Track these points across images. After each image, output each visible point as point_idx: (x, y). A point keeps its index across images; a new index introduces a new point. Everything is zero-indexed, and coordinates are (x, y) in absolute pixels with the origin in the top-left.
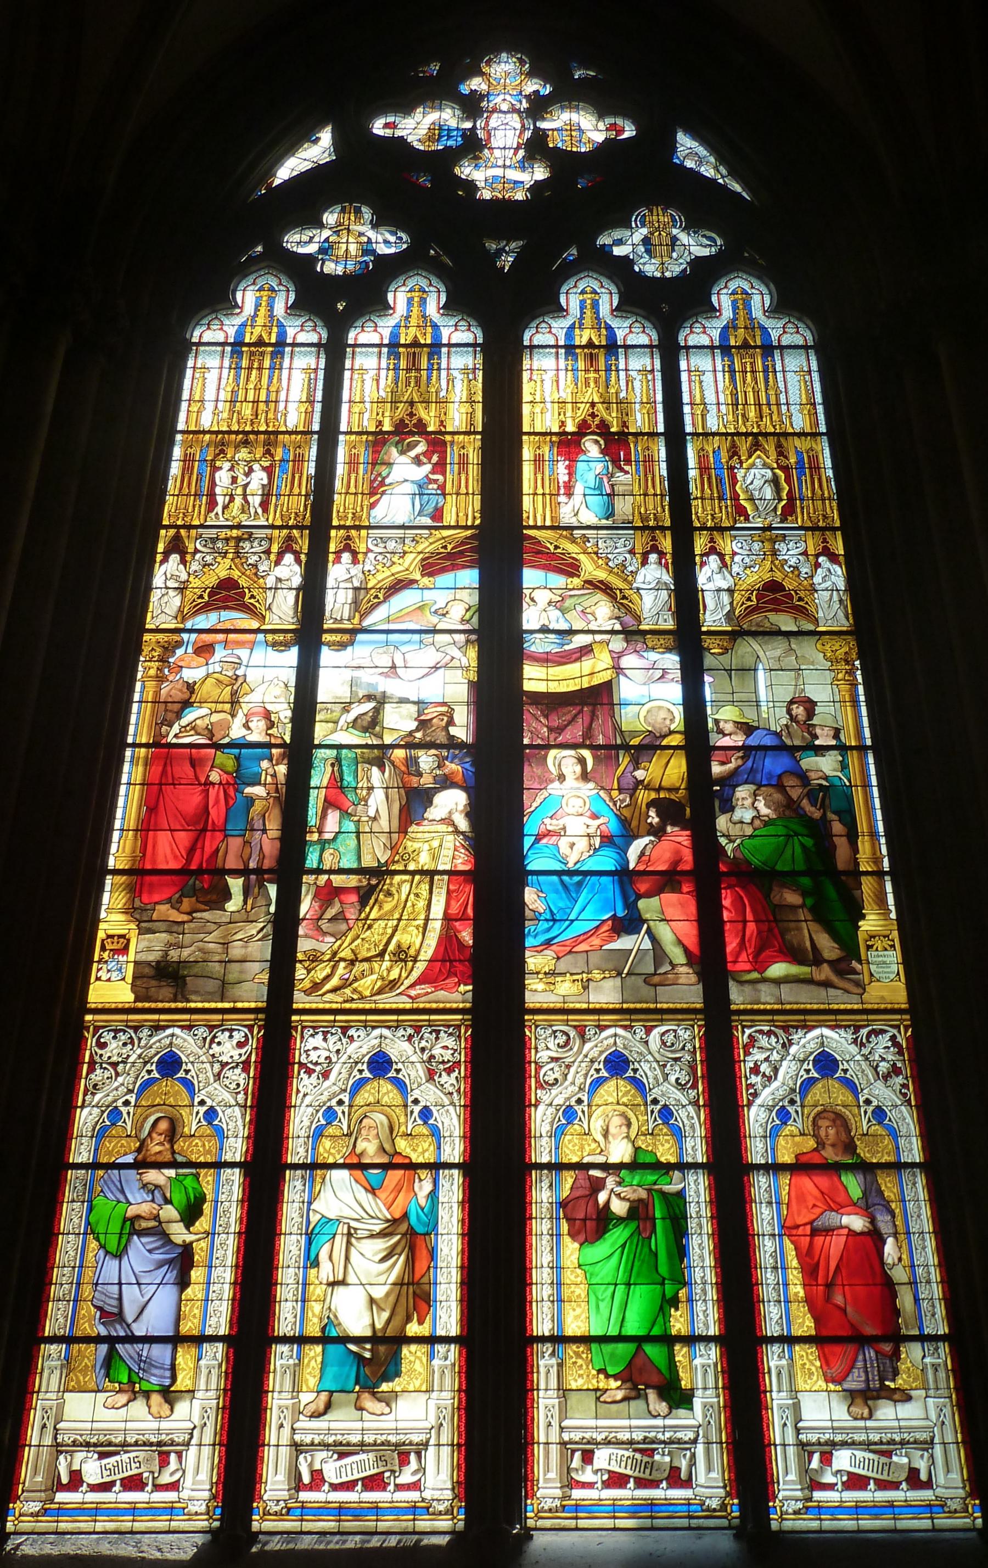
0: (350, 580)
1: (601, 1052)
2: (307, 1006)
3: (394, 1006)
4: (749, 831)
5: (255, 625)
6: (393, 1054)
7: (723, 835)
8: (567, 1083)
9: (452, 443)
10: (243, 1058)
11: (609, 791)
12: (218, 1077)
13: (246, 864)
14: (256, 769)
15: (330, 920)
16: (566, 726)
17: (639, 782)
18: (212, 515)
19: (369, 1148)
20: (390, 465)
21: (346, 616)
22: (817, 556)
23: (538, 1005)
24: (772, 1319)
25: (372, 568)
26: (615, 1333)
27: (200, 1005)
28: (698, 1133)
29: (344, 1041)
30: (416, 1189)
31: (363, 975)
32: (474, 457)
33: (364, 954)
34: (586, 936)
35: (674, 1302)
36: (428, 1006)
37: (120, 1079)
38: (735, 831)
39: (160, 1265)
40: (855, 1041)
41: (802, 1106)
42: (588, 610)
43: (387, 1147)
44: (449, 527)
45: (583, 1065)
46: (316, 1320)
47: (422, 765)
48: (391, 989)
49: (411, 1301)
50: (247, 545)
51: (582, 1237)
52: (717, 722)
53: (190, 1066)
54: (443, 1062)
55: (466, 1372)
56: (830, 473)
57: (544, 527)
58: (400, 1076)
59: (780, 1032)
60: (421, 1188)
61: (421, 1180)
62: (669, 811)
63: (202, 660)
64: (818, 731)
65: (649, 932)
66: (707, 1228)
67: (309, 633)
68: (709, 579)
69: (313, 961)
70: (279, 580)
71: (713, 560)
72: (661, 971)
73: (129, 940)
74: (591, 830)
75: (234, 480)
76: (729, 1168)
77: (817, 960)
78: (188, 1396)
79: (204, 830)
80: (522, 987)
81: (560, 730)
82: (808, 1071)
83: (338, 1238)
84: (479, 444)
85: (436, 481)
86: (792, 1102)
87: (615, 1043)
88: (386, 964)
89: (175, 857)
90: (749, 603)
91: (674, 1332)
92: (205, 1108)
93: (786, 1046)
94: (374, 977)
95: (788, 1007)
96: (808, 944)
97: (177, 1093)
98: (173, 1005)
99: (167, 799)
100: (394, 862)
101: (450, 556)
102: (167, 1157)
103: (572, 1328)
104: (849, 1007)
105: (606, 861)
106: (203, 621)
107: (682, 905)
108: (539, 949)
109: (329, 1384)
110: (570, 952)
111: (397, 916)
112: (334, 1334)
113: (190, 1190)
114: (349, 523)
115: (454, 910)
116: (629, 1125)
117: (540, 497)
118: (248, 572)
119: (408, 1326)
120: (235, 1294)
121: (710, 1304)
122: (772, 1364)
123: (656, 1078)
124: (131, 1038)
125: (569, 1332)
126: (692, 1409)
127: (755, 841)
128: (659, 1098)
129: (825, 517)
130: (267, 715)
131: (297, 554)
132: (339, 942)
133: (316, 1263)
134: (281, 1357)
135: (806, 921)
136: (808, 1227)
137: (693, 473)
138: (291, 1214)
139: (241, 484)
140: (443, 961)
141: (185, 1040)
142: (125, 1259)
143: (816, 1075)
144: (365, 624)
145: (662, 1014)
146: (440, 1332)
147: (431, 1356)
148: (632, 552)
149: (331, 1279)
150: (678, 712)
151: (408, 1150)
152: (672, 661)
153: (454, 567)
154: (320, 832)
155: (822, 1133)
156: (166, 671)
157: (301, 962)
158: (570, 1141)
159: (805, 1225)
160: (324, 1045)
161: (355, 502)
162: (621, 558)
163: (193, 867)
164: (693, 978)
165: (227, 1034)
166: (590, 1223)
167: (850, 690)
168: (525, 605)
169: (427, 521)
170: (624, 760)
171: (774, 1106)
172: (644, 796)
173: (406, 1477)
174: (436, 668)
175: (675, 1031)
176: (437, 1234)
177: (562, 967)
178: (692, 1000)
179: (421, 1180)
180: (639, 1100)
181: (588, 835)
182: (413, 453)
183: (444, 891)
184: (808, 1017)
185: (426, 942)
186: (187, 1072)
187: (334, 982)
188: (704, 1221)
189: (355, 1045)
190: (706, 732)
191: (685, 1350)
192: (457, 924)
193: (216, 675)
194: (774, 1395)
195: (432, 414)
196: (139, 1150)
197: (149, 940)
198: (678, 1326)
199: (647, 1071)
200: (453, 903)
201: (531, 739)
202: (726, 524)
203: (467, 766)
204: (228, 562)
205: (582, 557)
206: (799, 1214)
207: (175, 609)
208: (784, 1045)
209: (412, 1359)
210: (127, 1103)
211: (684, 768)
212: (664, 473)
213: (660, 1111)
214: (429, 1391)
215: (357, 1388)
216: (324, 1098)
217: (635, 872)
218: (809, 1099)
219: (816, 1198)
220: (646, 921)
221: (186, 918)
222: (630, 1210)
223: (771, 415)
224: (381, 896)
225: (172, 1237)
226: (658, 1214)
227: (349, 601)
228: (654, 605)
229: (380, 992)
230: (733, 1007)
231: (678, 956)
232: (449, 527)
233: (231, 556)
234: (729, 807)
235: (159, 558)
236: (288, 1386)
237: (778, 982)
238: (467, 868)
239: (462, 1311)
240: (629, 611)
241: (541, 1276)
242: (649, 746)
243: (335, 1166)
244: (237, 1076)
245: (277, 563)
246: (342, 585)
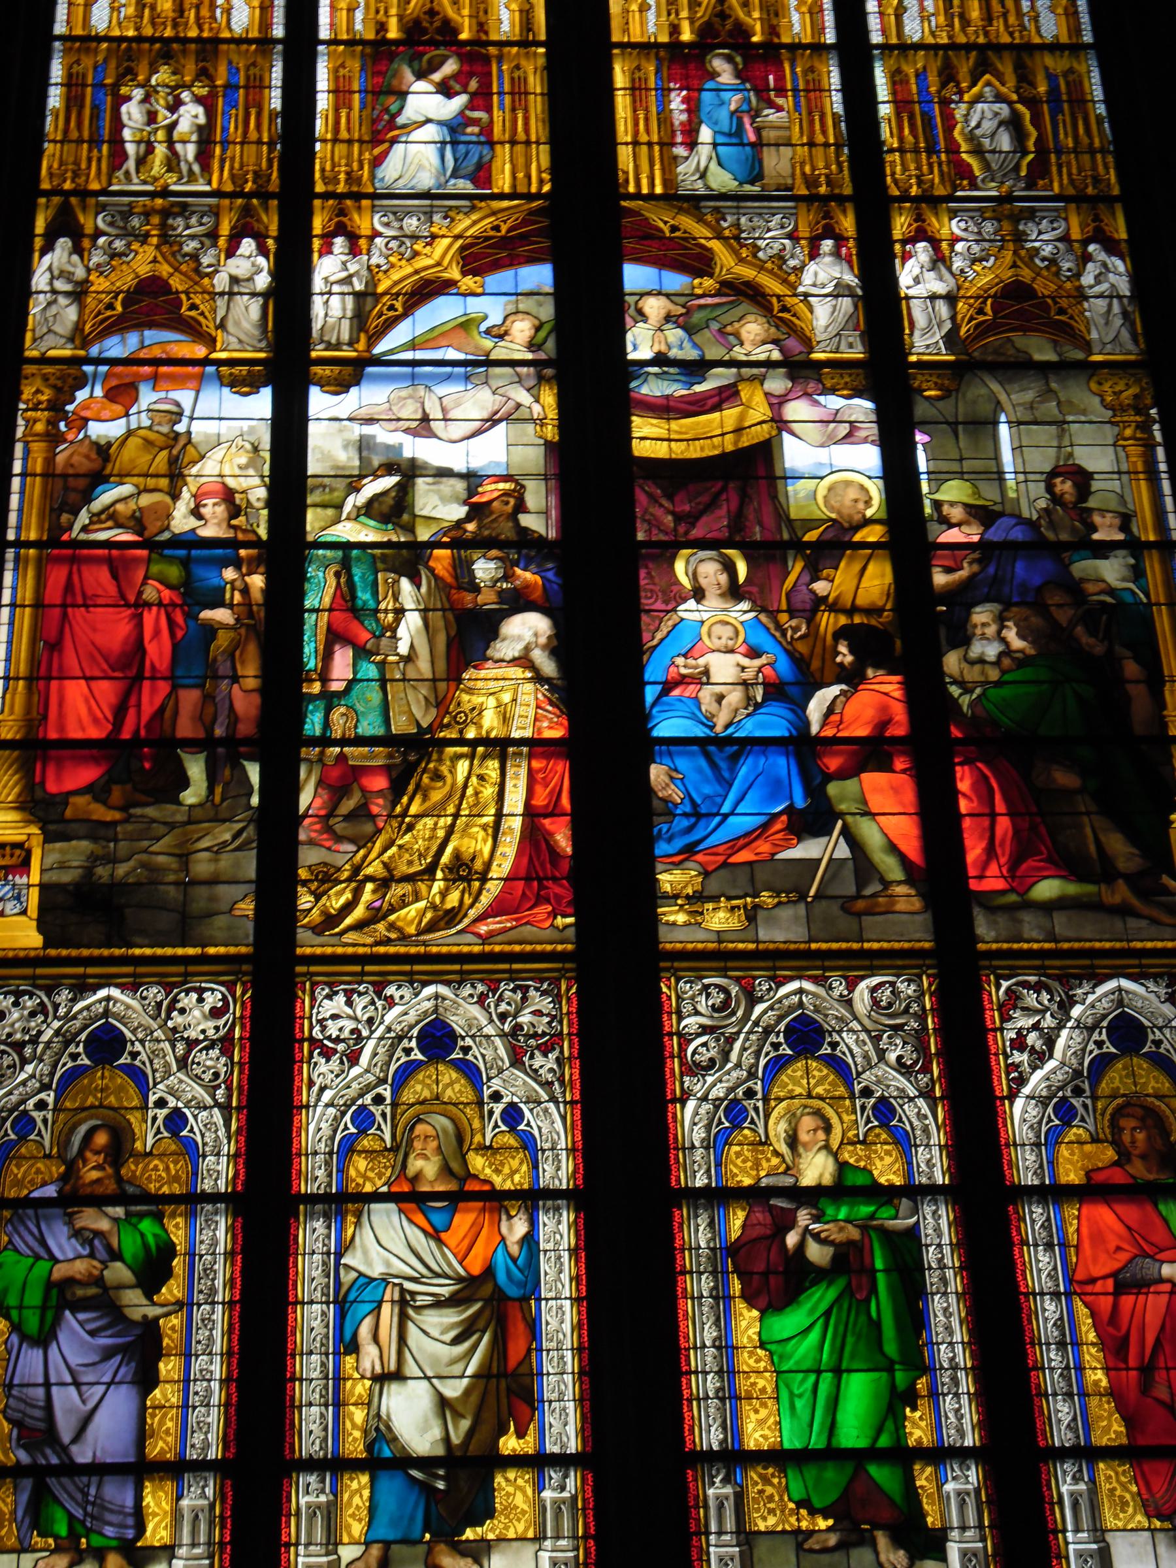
0: (347, 281)
1: (780, 1018)
2: (319, 951)
3: (455, 949)
4: (994, 674)
5: (200, 351)
6: (457, 1022)
7: (954, 682)
8: (729, 1065)
9: (500, 59)
10: (222, 1033)
11: (773, 614)
12: (183, 1063)
13: (210, 730)
14: (215, 581)
15: (348, 817)
16: (702, 513)
17: (819, 601)
18: (120, 174)
19: (426, 1166)
20: (403, 95)
21: (345, 336)
22: (1085, 243)
23: (679, 946)
25: (382, 261)
26: (821, 1445)
27: (148, 951)
28: (934, 1140)
29: (379, 1004)
30: (504, 1230)
31: (404, 904)
32: (536, 83)
33: (403, 869)
34: (748, 838)
35: (910, 1398)
36: (507, 948)
37: (29, 1068)
38: (972, 674)
39: (107, 1354)
41: (1095, 1098)
42: (729, 329)
43: (455, 1166)
44: (501, 196)
45: (753, 1037)
46: (357, 1434)
47: (479, 574)
48: (450, 924)
49: (504, 1401)
50: (179, 222)
51: (763, 1301)
52: (937, 505)
53: (138, 1047)
54: (535, 1036)
55: (596, 1509)
56: (1101, 109)
57: (651, 197)
58: (469, 1057)
59: (1055, 985)
60: (510, 1228)
61: (510, 1217)
62: (872, 644)
63: (119, 409)
64: (1097, 519)
66: (955, 1284)
67: (288, 366)
68: (917, 281)
69: (323, 882)
70: (234, 280)
71: (922, 250)
72: (868, 891)
73: (29, 853)
74: (749, 675)
75: (152, 117)
76: (983, 1191)
77: (1105, 872)
78: (164, 1555)
79: (139, 678)
80: (653, 920)
81: (692, 519)
82: (1099, 1044)
83: (386, 1309)
84: (541, 61)
85: (476, 122)
86: (1078, 1092)
87: (801, 1004)
88: (438, 885)
89: (96, 721)
90: (982, 318)
91: (911, 1442)
92: (165, 1111)
93: (1065, 1006)
94: (422, 904)
95: (1066, 945)
96: (1092, 848)
97: (121, 1088)
98: (106, 952)
99: (77, 629)
100: (442, 727)
101: (505, 243)
102: (111, 1187)
103: (756, 1436)
104: (1160, 945)
105: (773, 723)
106: (115, 347)
107: (896, 790)
109: (383, 1531)
110: (725, 865)
111: (451, 809)
112: (387, 1453)
113: (151, 1240)
114: (341, 188)
115: (540, 800)
116: (828, 1128)
117: (644, 148)
118: (184, 268)
119: (502, 1440)
120: (228, 1395)
121: (965, 1400)
122: (1064, 1489)
123: (866, 1056)
124: (42, 1003)
125: (751, 1444)
127: (1005, 691)
128: (874, 1087)
129: (1096, 180)
130: (228, 495)
131: (260, 239)
132: (362, 852)
133: (353, 1347)
134: (307, 1494)
135: (1088, 814)
136: (1110, 1283)
137: (885, 110)
138: (309, 1271)
139: (162, 121)
140: (528, 879)
141: (128, 1007)
142: (53, 1350)
143: (1113, 1050)
144: (378, 349)
145: (871, 962)
146: (552, 1448)
147: (539, 1487)
148: (793, 236)
149: (378, 1369)
150: (876, 490)
151: (488, 1171)
153: (514, 261)
154: (325, 678)
155: (1126, 1137)
156: (62, 426)
157: (305, 883)
158: (738, 1154)
159: (1105, 1277)
160: (349, 1011)
161: (349, 155)
162: (777, 246)
163: (126, 735)
164: (917, 904)
165: (194, 996)
166: (773, 1278)
167: (1144, 455)
168: (629, 321)
169: (464, 186)
170: (797, 568)
171: (1050, 1098)
172: (828, 622)
174: (492, 421)
175: (893, 984)
176: (539, 1300)
177: (713, 887)
178: (918, 936)
179: (510, 1217)
180: (842, 1090)
181: (744, 683)
182: (437, 77)
183: (523, 772)
184: (1097, 962)
185: (500, 850)
186: (134, 1055)
187: (359, 912)
188: (950, 1274)
189: (397, 1010)
190: (920, 520)
191: (929, 1470)
192: (546, 822)
193: (141, 432)
194: (1070, 1535)
195: (466, 12)
196: (64, 1178)
197: (61, 851)
198: (918, 1433)
199: (852, 1044)
200: (539, 789)
201: (649, 532)
202: (940, 191)
203: (550, 575)
204: (149, 252)
205: (715, 245)
206: (1095, 1260)
207: (69, 326)
208: (1061, 1005)
209: (511, 1489)
210: (41, 1105)
211: (889, 578)
212: (839, 108)
213: (874, 1107)
214: (539, 1538)
215: (428, 1536)
216: (352, 1092)
217: (820, 740)
218: (1104, 1087)
219: (1120, 1237)
220: (841, 815)
221: (117, 815)
222: (835, 1258)
223: (1005, 15)
224: (426, 779)
225: (127, 1311)
226: (879, 1264)
227: (349, 314)
229: (432, 927)
230: (981, 946)
231: (892, 868)
232: (501, 196)
233: (155, 240)
234: (962, 638)
235: (38, 243)
236: (319, 1535)
237: (1049, 907)
238: (557, 734)
239: (583, 1415)
240: (793, 330)
241: (702, 1359)
242: (835, 543)
243: (376, 1197)
244: (211, 1060)
245: (231, 253)
246: (336, 288)
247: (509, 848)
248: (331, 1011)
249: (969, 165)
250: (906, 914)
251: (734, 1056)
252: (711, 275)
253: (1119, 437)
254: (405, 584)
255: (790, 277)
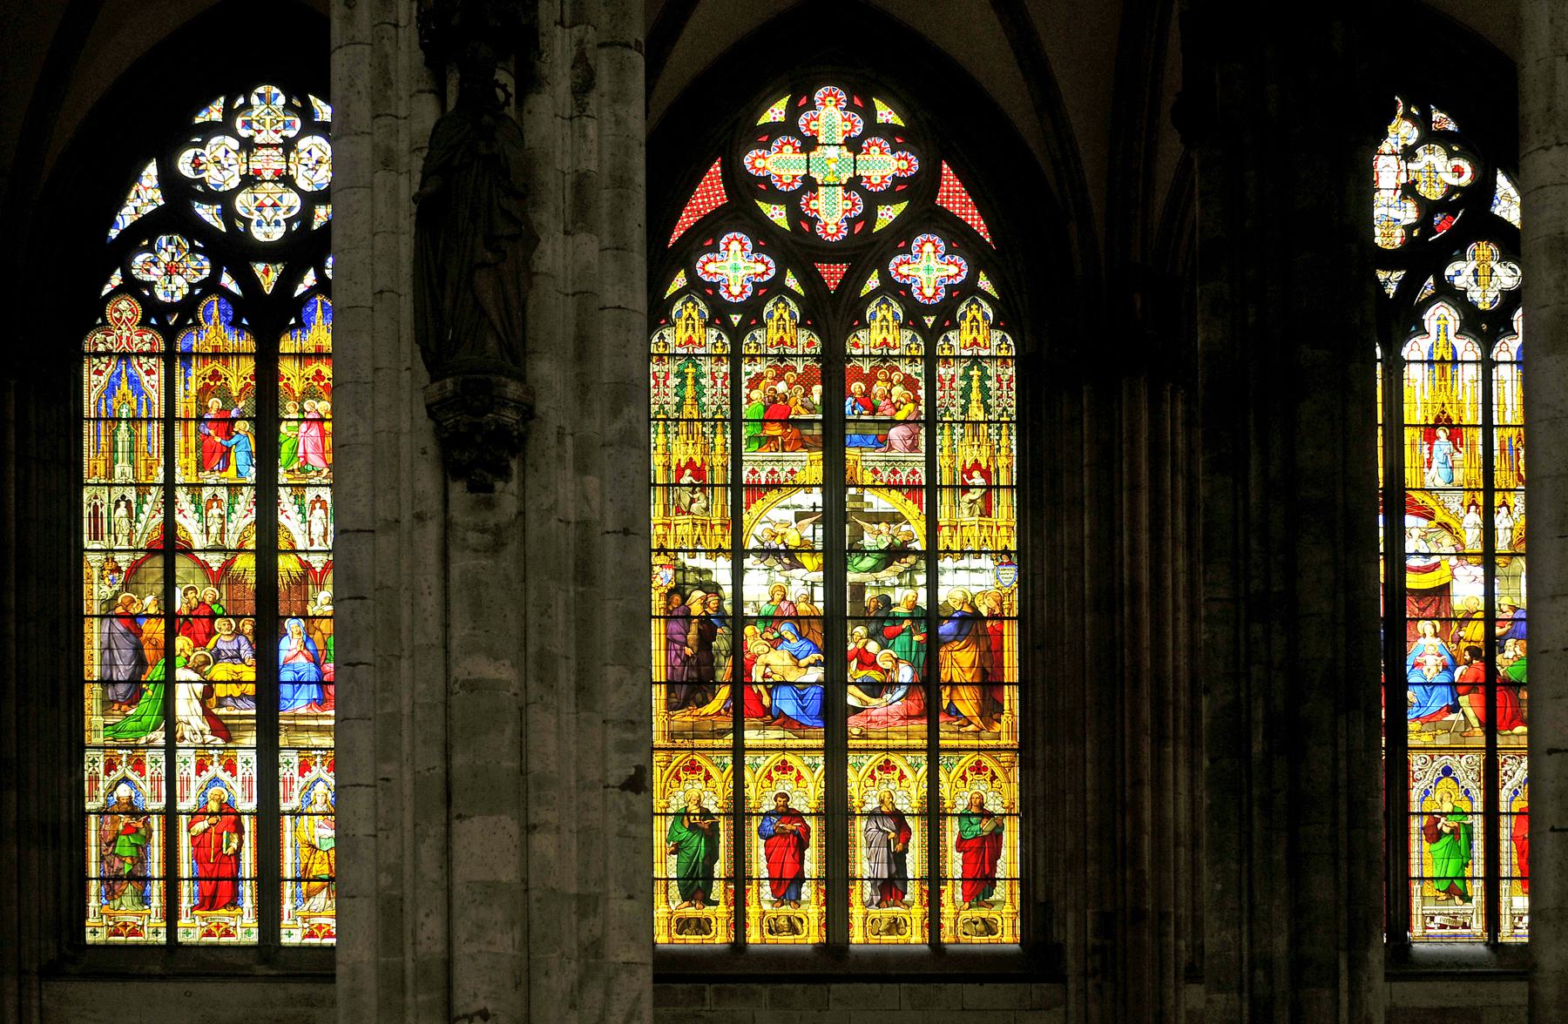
24: (1504, 871)
38: (1504, 663)
105: (1444, 678)
108: (1413, 720)
152: (1480, 571)
166: (1433, 835)
170: (1455, 625)
172: (1463, 645)
199: (1459, 774)
228: (1472, 539)
231: (1475, 723)
250: (1479, 738)
255: (1460, 520)
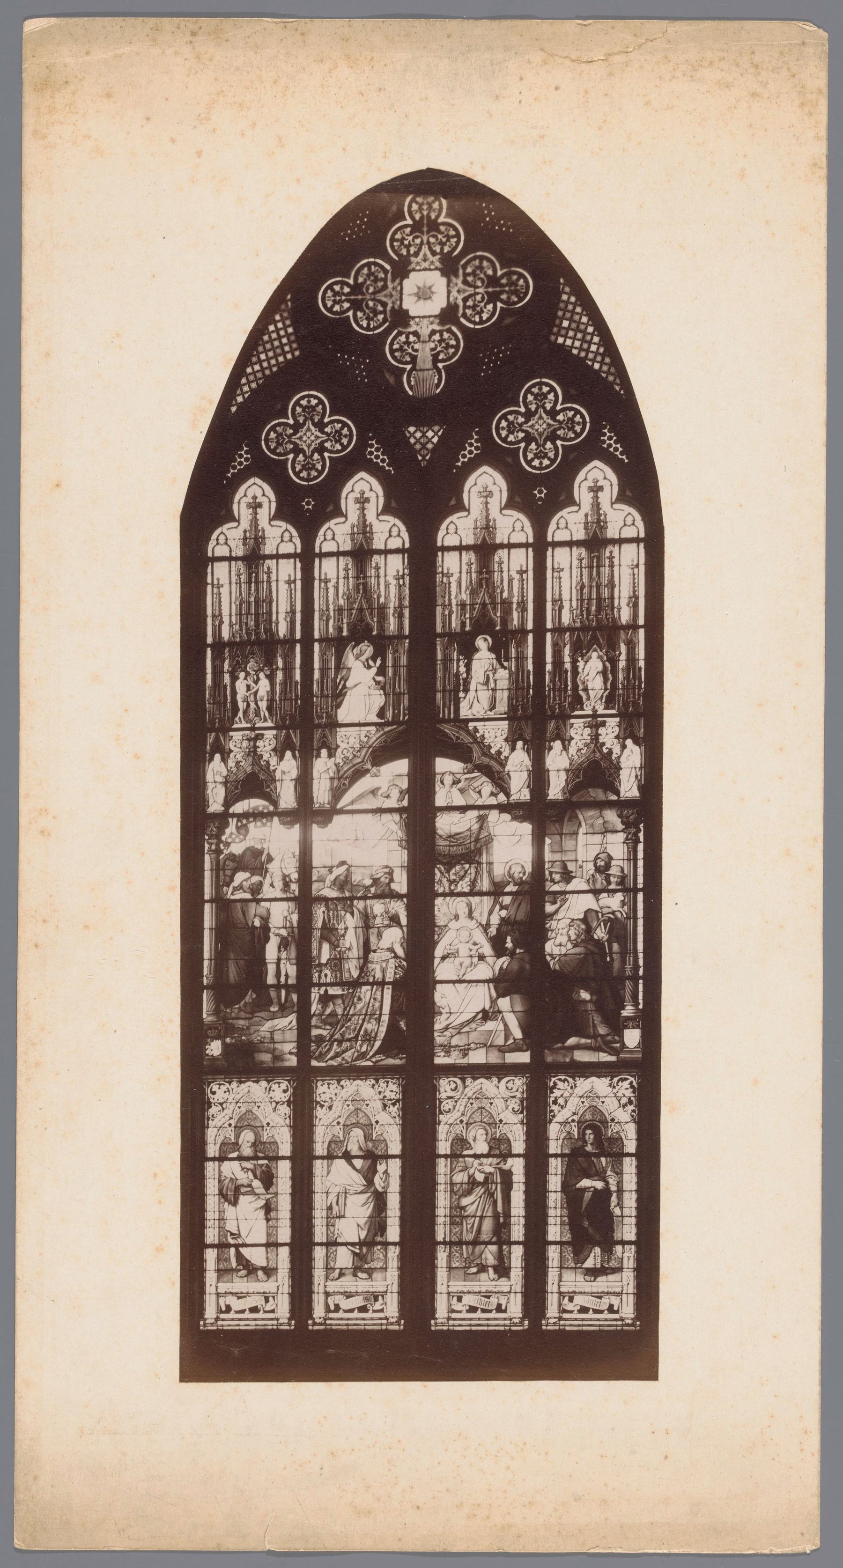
12: (275, 1110)
18: (237, 719)
33: (347, 1036)
38: (556, 951)
40: (610, 1086)
54: (391, 1100)
57: (449, 721)
59: (570, 1080)
65: (503, 1019)
70: (283, 773)
74: (473, 953)
75: (248, 688)
88: (359, 1042)
94: (353, 1050)
106: (240, 807)
111: (364, 1012)
126: (509, 1278)
156: (221, 845)
173: (378, 1306)
182: (363, 658)
187: (332, 1054)
208: (572, 1087)
216: (331, 1120)
224: (355, 1000)
247: (383, 1029)
248: (324, 1090)
249: (581, 697)
251: (457, 1108)
252: (471, 762)
253: (627, 839)
254: (348, 915)
